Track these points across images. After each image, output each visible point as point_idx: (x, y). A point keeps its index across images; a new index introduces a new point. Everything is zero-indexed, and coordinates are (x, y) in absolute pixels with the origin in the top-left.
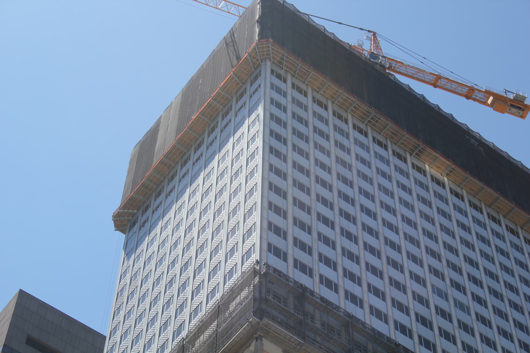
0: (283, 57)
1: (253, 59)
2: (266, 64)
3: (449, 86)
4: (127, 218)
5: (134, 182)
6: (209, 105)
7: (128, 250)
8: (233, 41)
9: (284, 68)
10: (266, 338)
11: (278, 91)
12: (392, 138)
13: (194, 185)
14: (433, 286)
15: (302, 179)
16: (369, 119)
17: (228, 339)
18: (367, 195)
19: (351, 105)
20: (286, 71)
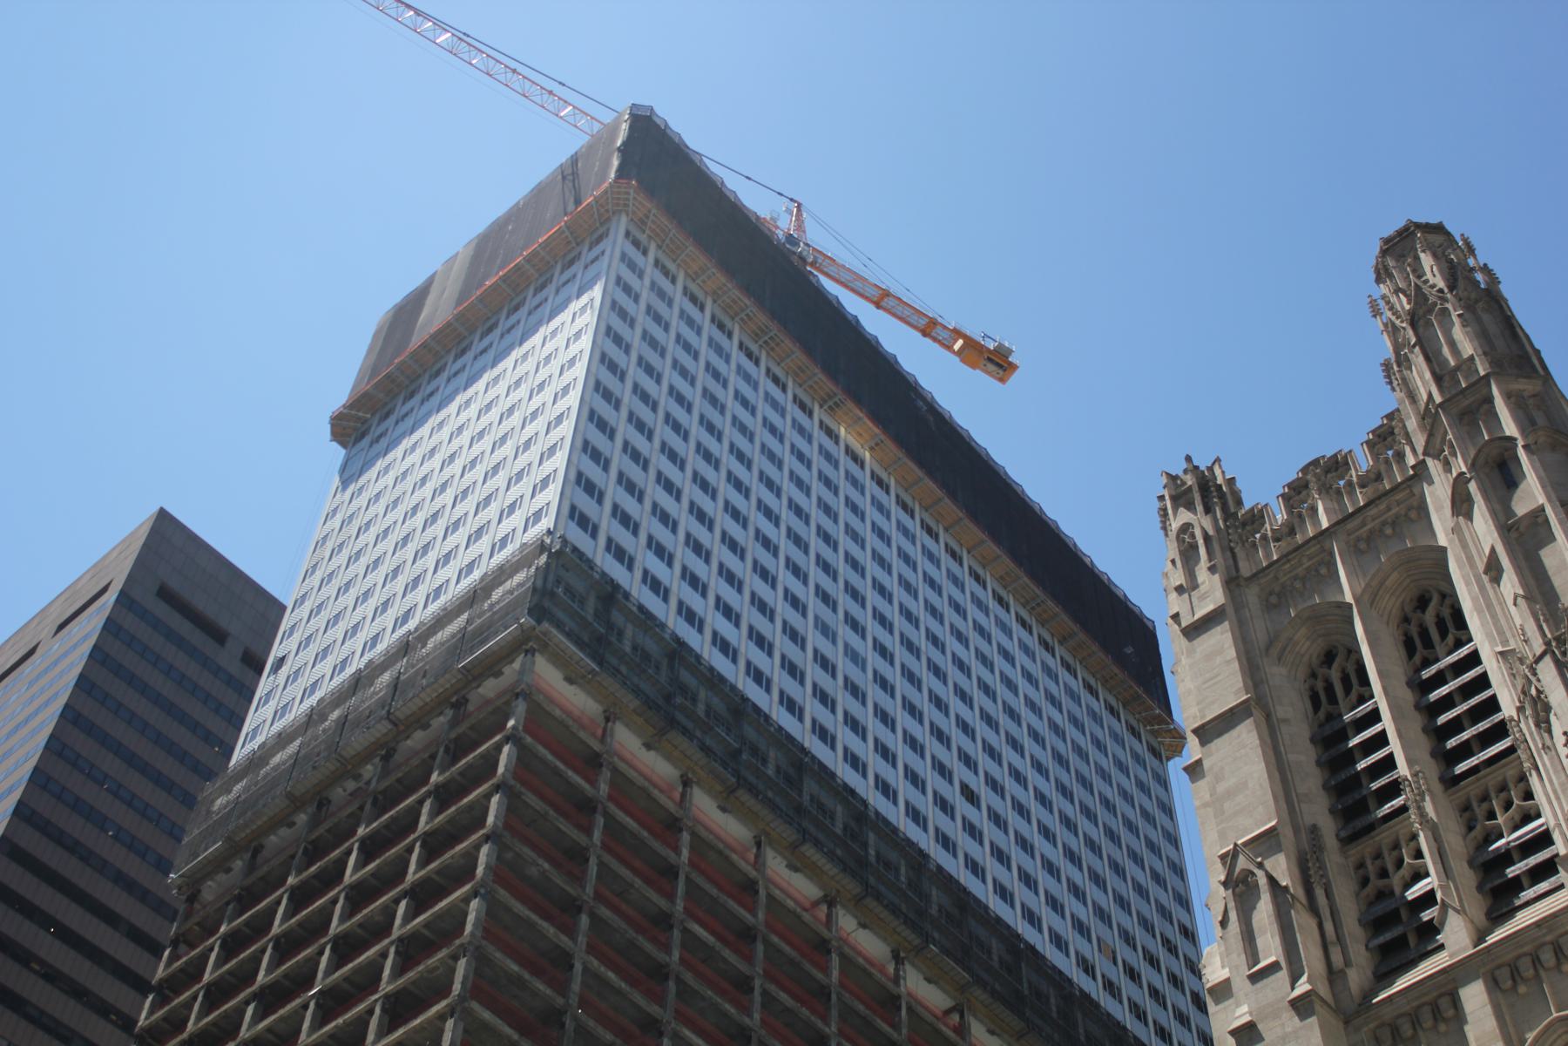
2: (619, 220)
3: (899, 310)
4: (352, 424)
5: (375, 370)
6: (518, 268)
7: (346, 476)
8: (575, 174)
9: (647, 232)
10: (541, 653)
11: (632, 266)
12: (797, 375)
13: (471, 391)
14: (816, 618)
15: (644, 413)
16: (766, 338)
18: (741, 457)
19: (743, 310)
20: (650, 237)
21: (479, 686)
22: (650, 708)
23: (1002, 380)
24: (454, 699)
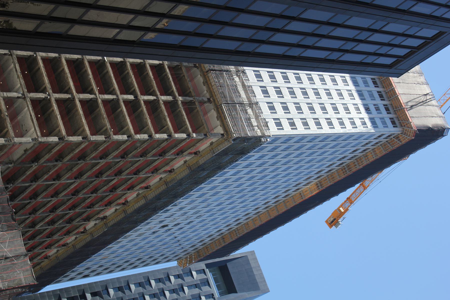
0: (400, 141)
1: (406, 123)
9: (393, 138)
17: (230, 115)
21: (214, 110)
22: (198, 167)
23: (327, 222)
24: (211, 99)
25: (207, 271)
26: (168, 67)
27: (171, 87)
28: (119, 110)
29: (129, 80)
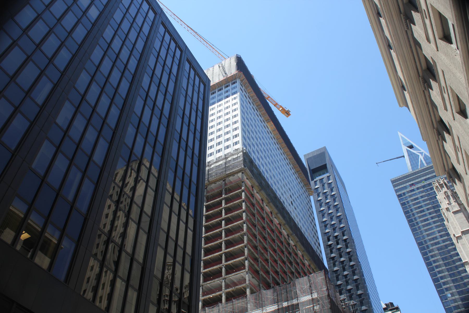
23: (287, 117)
25: (315, 180)
26: (207, 203)
27: (218, 201)
28: (230, 228)
29: (214, 224)
